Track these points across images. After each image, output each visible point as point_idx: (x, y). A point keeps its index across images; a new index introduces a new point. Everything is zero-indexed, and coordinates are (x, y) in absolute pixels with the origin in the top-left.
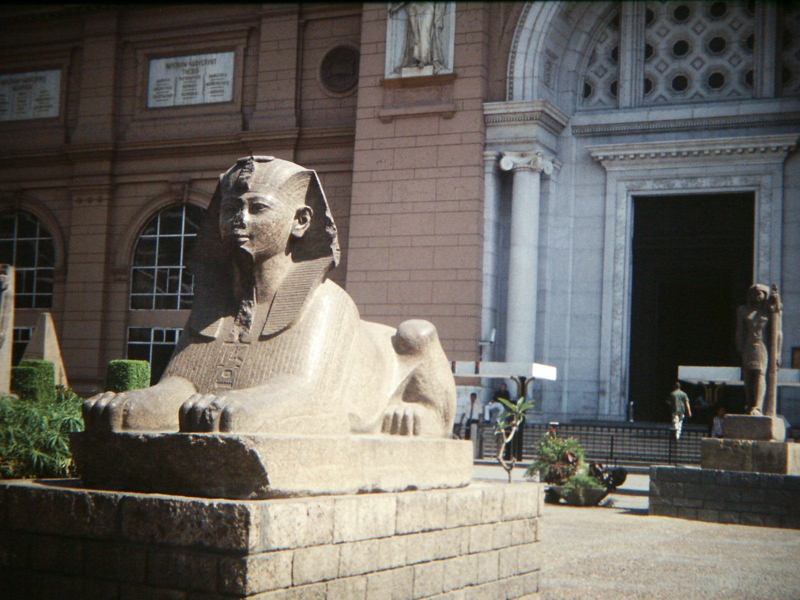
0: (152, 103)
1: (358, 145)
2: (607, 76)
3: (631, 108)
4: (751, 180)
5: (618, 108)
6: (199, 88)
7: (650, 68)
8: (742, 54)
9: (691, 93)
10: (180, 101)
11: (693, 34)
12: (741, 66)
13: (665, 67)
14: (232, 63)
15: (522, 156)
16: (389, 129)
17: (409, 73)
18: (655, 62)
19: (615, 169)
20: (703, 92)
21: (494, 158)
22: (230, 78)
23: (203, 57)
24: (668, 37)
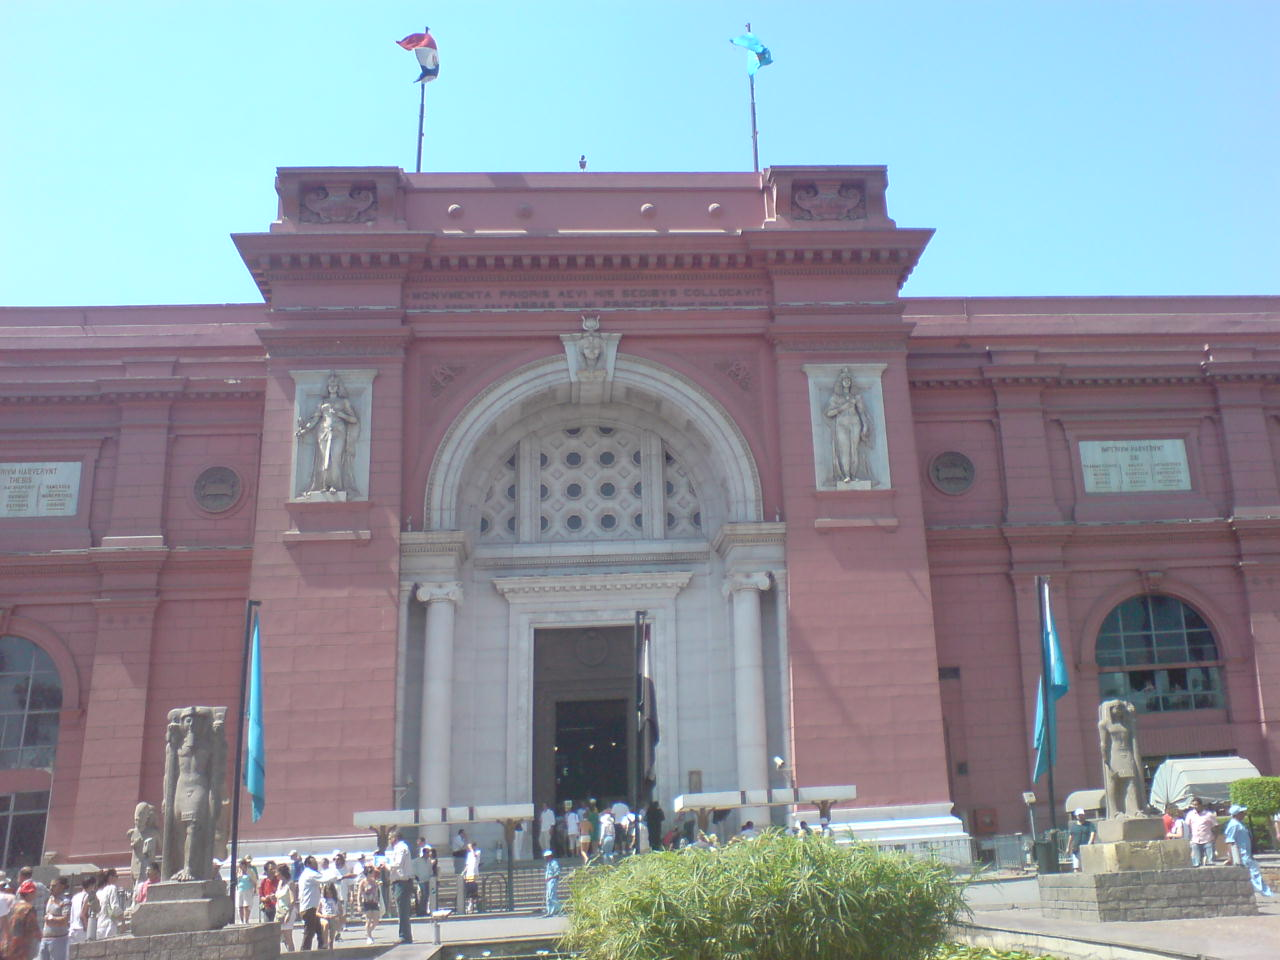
1: (255, 573)
2: (504, 512)
3: (530, 543)
5: (517, 543)
6: (32, 500)
7: (547, 505)
8: (631, 498)
9: (585, 532)
12: (631, 510)
13: (560, 507)
14: (78, 474)
15: (440, 587)
17: (316, 496)
20: (598, 531)
21: (410, 588)
22: (74, 489)
23: (38, 465)
24: (562, 480)
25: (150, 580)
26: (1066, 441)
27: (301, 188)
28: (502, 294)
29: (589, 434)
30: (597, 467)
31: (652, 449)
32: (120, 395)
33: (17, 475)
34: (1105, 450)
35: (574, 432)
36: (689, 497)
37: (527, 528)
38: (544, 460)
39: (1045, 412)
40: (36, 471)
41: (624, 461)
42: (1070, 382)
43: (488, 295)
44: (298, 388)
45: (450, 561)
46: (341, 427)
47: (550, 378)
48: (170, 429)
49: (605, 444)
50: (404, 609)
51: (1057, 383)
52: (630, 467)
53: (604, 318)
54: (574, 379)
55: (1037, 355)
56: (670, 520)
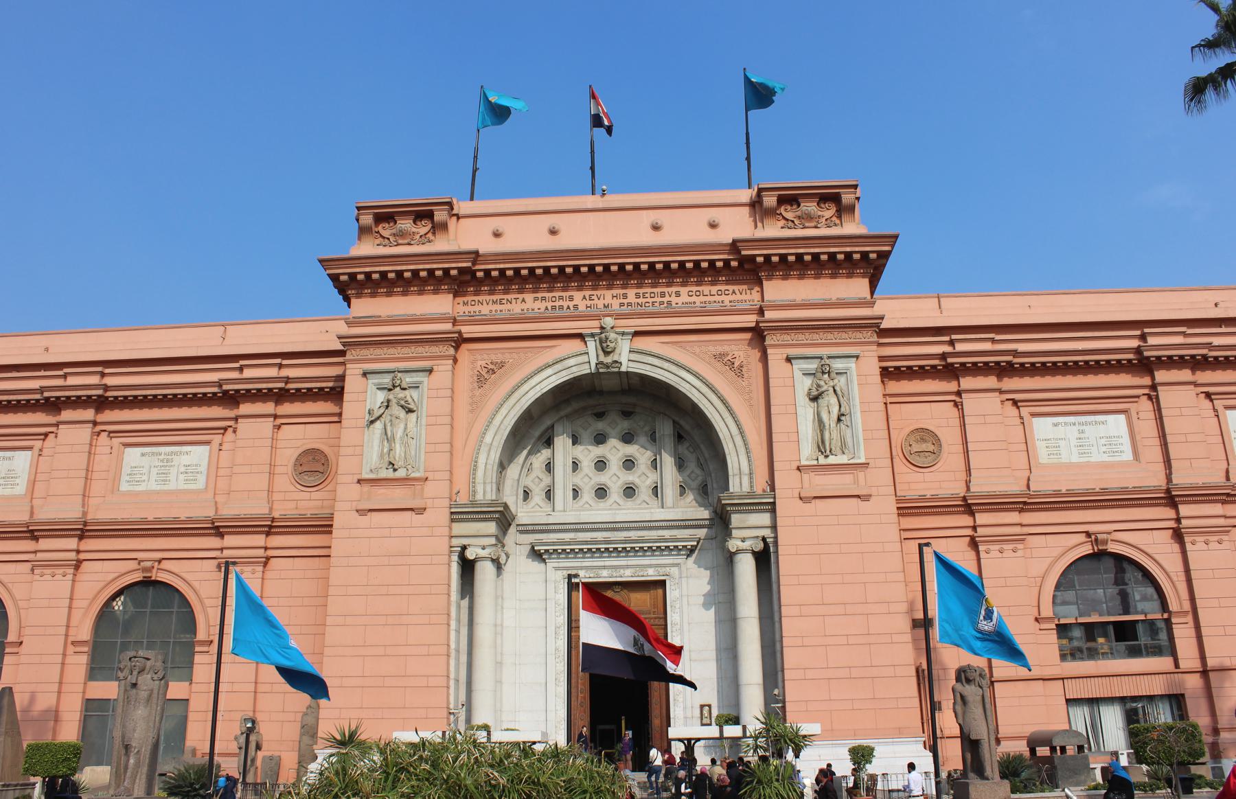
0: (124, 487)
4: (662, 571)
6: (172, 477)
7: (578, 479)
10: (153, 486)
11: (609, 456)
13: (588, 478)
16: (365, 520)
17: (384, 474)
18: (580, 476)
22: (204, 468)
25: (260, 540)
26: (1021, 418)
28: (536, 299)
31: (665, 429)
32: (237, 391)
33: (162, 457)
34: (1056, 425)
35: (600, 416)
36: (698, 471)
38: (575, 441)
39: (1001, 392)
40: (176, 453)
42: (1022, 365)
43: (523, 300)
44: (370, 381)
45: (491, 527)
46: (402, 414)
47: (574, 369)
49: (625, 425)
50: (455, 568)
51: (1010, 363)
55: (993, 341)
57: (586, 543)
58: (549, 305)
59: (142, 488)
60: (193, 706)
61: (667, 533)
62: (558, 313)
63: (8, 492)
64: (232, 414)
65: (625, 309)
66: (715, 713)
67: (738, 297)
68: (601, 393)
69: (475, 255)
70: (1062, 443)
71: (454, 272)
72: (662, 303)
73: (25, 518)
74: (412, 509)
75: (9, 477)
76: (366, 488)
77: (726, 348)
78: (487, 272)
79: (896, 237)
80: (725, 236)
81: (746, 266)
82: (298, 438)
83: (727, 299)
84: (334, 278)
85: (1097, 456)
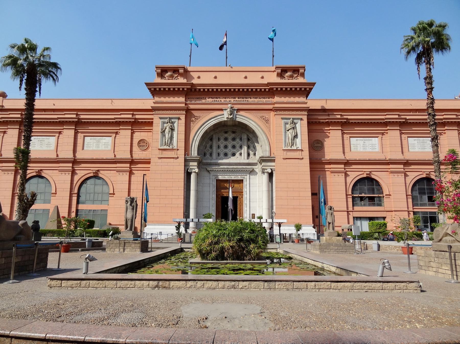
6: (100, 146)
7: (219, 151)
10: (94, 148)
13: (222, 151)
17: (165, 147)
19: (212, 173)
25: (128, 165)
27: (162, 72)
28: (209, 98)
29: (230, 133)
30: (231, 141)
34: (357, 140)
35: (226, 132)
36: (253, 149)
37: (214, 155)
40: (101, 139)
41: (238, 140)
48: (132, 130)
49: (233, 135)
52: (239, 141)
53: (233, 104)
54: (226, 120)
56: (249, 155)
57: (222, 168)
58: (213, 100)
59: (91, 149)
60: (108, 211)
61: (244, 167)
62: (216, 102)
63: (49, 149)
64: (118, 128)
65: (235, 102)
66: (256, 216)
67: (268, 100)
68: (227, 126)
69: (192, 85)
70: (358, 145)
71: (185, 89)
72: (246, 101)
73: (55, 156)
74: (173, 158)
75: (48, 144)
76: (161, 151)
77: (263, 115)
78: (195, 89)
79: (315, 83)
80: (265, 81)
81: (271, 91)
82: (138, 136)
83: (264, 100)
84: (150, 89)
85: (368, 150)
